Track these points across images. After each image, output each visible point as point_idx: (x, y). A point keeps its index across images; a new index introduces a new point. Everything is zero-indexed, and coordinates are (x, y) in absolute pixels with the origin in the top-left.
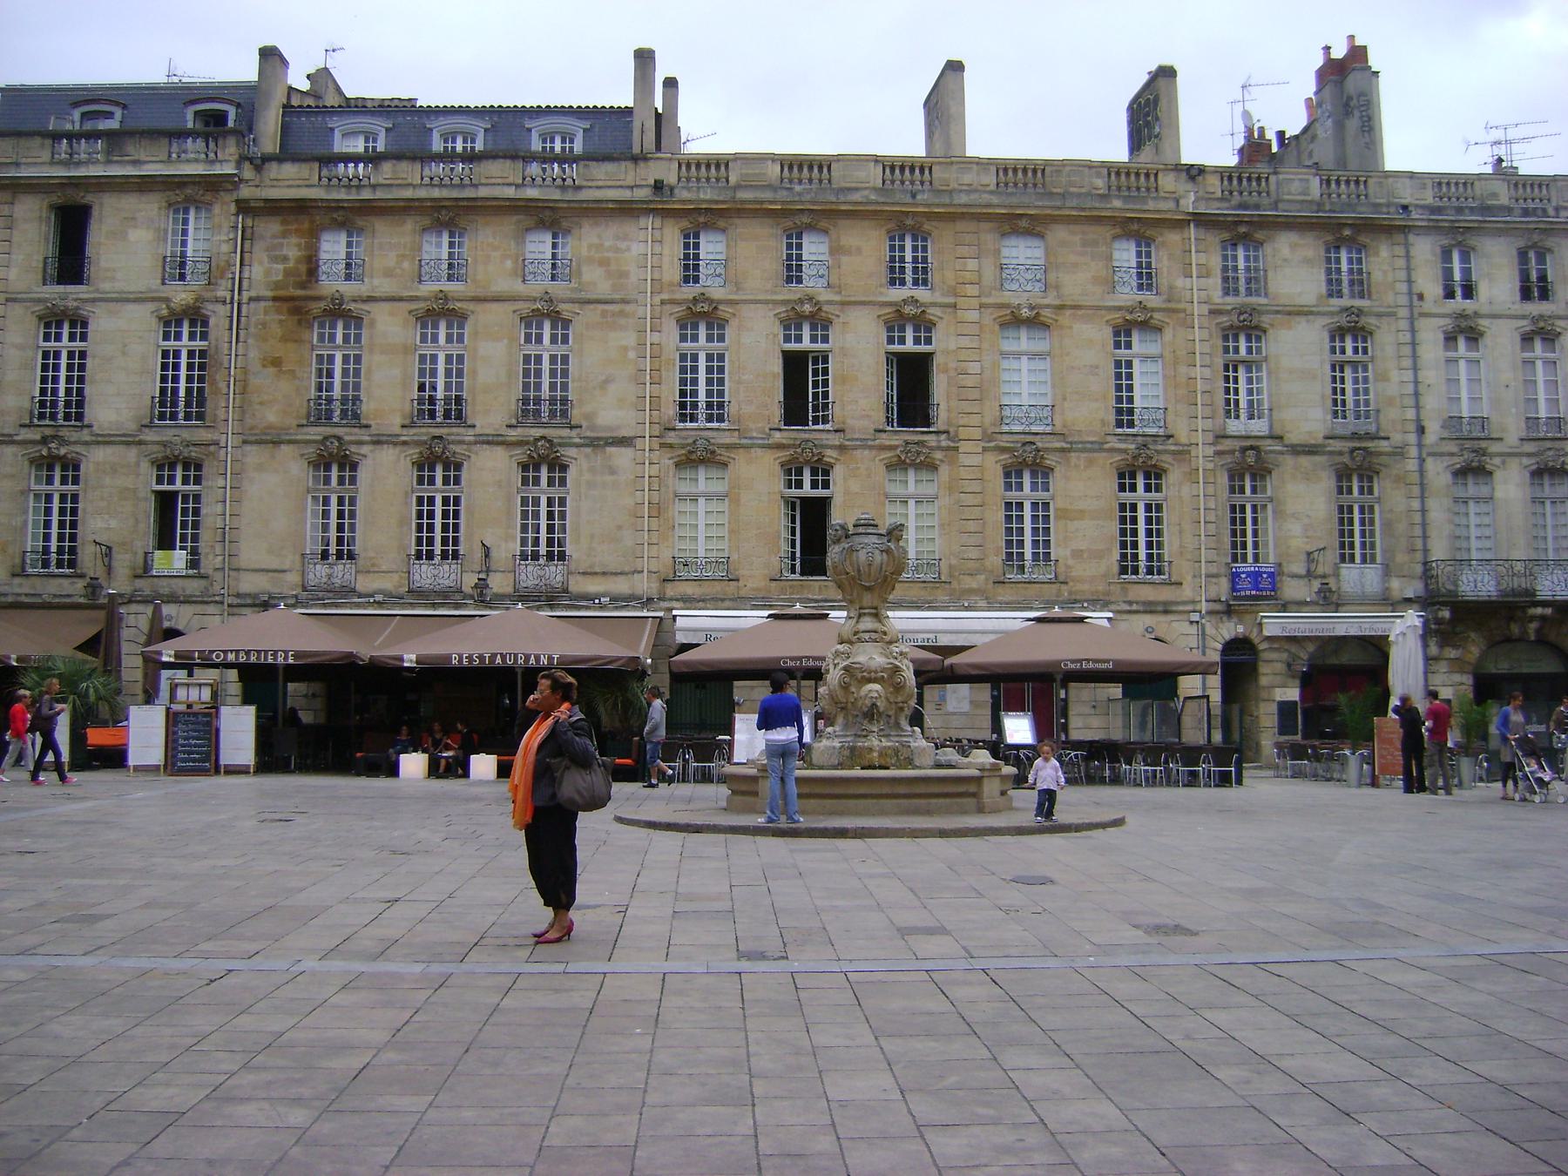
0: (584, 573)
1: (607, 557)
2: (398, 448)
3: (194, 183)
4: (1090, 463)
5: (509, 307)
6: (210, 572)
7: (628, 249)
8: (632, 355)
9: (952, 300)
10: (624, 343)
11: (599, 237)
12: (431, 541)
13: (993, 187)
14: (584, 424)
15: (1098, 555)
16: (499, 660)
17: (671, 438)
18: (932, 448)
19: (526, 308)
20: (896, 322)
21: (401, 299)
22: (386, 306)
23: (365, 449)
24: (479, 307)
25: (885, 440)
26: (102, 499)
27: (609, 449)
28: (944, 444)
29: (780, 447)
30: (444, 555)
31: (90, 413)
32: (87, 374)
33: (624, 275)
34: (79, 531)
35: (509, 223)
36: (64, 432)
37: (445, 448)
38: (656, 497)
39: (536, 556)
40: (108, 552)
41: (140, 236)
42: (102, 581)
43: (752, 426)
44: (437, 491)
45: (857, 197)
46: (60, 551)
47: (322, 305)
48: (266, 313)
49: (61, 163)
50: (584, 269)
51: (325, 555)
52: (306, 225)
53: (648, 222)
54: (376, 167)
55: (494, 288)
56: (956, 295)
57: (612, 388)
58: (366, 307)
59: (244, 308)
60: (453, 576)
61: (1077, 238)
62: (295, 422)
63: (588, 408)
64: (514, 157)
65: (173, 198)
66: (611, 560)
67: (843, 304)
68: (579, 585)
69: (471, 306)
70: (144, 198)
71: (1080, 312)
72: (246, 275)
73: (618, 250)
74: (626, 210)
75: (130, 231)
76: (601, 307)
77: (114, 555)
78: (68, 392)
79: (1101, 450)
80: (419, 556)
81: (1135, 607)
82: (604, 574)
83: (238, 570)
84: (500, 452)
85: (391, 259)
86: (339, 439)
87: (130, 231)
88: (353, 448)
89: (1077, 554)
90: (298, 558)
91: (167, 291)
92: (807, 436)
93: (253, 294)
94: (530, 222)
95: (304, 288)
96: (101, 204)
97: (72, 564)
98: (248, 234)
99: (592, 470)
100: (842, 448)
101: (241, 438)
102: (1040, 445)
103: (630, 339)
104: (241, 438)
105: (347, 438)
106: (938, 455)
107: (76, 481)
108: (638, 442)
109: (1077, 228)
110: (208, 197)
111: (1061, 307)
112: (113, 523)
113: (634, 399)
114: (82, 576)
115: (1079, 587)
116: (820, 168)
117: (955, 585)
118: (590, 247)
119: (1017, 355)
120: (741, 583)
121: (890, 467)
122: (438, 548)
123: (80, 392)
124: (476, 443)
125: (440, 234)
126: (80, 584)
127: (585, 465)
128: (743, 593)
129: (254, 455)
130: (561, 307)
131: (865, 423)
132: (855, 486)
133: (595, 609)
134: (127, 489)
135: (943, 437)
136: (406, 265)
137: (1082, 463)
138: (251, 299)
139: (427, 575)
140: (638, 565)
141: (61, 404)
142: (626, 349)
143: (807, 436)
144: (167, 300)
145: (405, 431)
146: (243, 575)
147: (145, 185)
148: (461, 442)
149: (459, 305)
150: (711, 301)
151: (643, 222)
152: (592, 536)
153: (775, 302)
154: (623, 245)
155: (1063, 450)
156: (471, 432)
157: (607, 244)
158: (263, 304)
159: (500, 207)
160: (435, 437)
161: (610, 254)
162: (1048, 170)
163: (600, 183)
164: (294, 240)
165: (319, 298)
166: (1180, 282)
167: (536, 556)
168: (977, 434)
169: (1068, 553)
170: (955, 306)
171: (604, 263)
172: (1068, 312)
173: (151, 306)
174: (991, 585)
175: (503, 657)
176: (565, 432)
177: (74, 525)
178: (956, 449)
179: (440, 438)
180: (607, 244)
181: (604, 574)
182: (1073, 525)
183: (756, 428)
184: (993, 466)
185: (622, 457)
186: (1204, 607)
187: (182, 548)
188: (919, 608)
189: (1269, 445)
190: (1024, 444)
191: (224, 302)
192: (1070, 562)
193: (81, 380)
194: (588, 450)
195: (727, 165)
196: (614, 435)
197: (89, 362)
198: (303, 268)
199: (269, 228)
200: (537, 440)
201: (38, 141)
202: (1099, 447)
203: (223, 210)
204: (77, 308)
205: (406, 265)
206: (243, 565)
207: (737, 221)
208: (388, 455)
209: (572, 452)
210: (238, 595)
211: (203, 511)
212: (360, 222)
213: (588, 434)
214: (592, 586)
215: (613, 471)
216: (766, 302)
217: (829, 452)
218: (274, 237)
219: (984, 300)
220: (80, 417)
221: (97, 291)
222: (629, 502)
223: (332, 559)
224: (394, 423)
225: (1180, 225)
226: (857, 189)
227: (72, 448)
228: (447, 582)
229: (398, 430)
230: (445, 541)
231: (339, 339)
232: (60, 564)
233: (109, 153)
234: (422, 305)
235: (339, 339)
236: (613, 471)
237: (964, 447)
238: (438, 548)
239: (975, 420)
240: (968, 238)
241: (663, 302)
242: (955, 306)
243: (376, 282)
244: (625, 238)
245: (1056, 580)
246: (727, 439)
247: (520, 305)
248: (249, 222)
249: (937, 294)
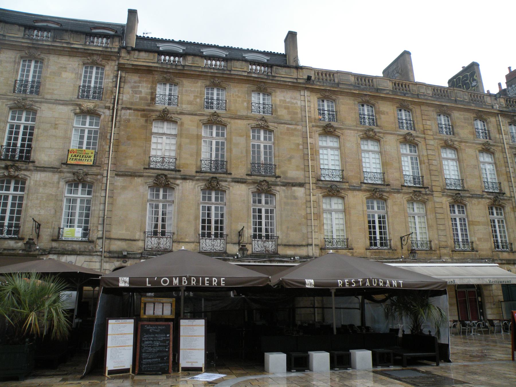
0: (285, 245)
1: (295, 237)
2: (194, 182)
3: (97, 54)
5: (245, 122)
6: (95, 239)
7: (297, 103)
8: (301, 147)
9: (423, 136)
10: (297, 142)
11: (284, 97)
12: (209, 228)
13: (431, 95)
14: (282, 176)
16: (368, 284)
18: (423, 194)
19: (254, 123)
21: (196, 115)
22: (190, 117)
23: (178, 182)
24: (232, 121)
26: (37, 199)
27: (294, 188)
28: (428, 192)
30: (216, 235)
31: (34, 156)
32: (34, 137)
33: (296, 113)
34: (22, 216)
35: (245, 87)
36: (19, 164)
37: (218, 183)
39: (260, 237)
40: (39, 226)
41: (68, 76)
42: (35, 240)
43: (353, 181)
44: (213, 204)
46: (10, 226)
47: (158, 114)
48: (130, 115)
49: (27, 39)
50: (278, 110)
51: (155, 233)
52: (151, 79)
54: (184, 59)
55: (239, 114)
56: (424, 134)
57: (293, 161)
58: (179, 116)
59: (119, 112)
60: (222, 245)
61: (462, 117)
62: (143, 167)
63: (283, 169)
64: (155, 52)
65: (86, 61)
67: (384, 133)
68: (282, 251)
69: (229, 120)
70: (71, 59)
71: (467, 144)
72: (121, 98)
73: (292, 103)
75: (63, 73)
76: (287, 126)
77: (41, 229)
78: (22, 145)
79: (482, 198)
80: (203, 235)
81: (503, 262)
82: (294, 246)
83: (110, 239)
84: (243, 187)
85: (191, 98)
86: (166, 176)
87: (63, 73)
88: (172, 181)
89: (479, 239)
90: (142, 234)
91: (80, 102)
92: (376, 186)
93: (124, 106)
94: (254, 88)
95: (149, 106)
96: (49, 59)
97: (16, 232)
98: (123, 80)
99: (286, 197)
101: (115, 173)
102: (462, 195)
103: (300, 141)
104: (115, 173)
105: (169, 176)
107: (23, 189)
108: (307, 186)
109: (462, 113)
110: (104, 62)
111: (461, 142)
112: (42, 212)
113: (303, 167)
114: (22, 239)
116: (330, 75)
117: (438, 252)
118: (280, 101)
119: (368, 151)
120: (354, 251)
122: (213, 232)
123: (29, 146)
124: (232, 181)
125: (165, 84)
126: (20, 244)
127: (283, 195)
129: (120, 181)
131: (397, 182)
132: (396, 209)
133: (291, 262)
134: (51, 194)
135: (427, 190)
136: (198, 100)
137: (476, 203)
138: (122, 108)
139: (207, 244)
140: (310, 242)
141: (18, 151)
142: (298, 145)
143: (376, 186)
144: (80, 105)
145: (198, 174)
146: (113, 242)
147: (73, 53)
148: (226, 181)
149: (223, 119)
150: (375, 132)
151: (302, 93)
152: (288, 228)
153: (358, 130)
154: (295, 101)
155: (469, 197)
156: (229, 176)
157: (287, 100)
158: (128, 111)
159: (279, 84)
160: (213, 178)
161: (289, 105)
162: (374, 80)
163: (283, 76)
164: (145, 85)
165: (156, 111)
166: (498, 136)
167: (260, 237)
169: (476, 239)
171: (287, 108)
172: (463, 144)
173: (71, 107)
174: (451, 253)
175: (371, 282)
176: (273, 179)
177: (19, 212)
178: (432, 195)
179: (216, 178)
180: (287, 100)
181: (294, 246)
182: (476, 228)
184: (446, 201)
185: (300, 192)
187: (79, 227)
188: (426, 262)
189: (462, 194)
190: (456, 194)
191: (109, 108)
192: (478, 243)
193: (30, 140)
194: (284, 188)
195: (333, 75)
196: (295, 181)
197: (36, 131)
198: (149, 97)
199: (133, 78)
200: (261, 181)
201: (17, 27)
202: (482, 197)
203: (110, 68)
204: (32, 105)
205: (198, 100)
206: (113, 236)
207: (340, 97)
208: (189, 185)
209: (278, 188)
210: (110, 252)
211: (92, 208)
212: (177, 80)
213: (284, 180)
214: (290, 252)
216: (354, 130)
217: (385, 194)
218: (135, 82)
219: (435, 137)
220: (28, 158)
221: (43, 98)
222: (303, 213)
223: (159, 235)
224: (191, 171)
225: (495, 115)
226: (384, 90)
227: (23, 172)
228: (219, 248)
229: (194, 174)
230: (216, 228)
231: (262, 138)
232: (9, 232)
233: (54, 38)
234: (206, 118)
235: (262, 138)
236: (295, 198)
237: (435, 194)
238: (213, 232)
241: (313, 126)
242: (425, 138)
243: (184, 106)
244: (295, 99)
245: (473, 250)
247: (251, 122)
248: (124, 75)
249: (418, 133)
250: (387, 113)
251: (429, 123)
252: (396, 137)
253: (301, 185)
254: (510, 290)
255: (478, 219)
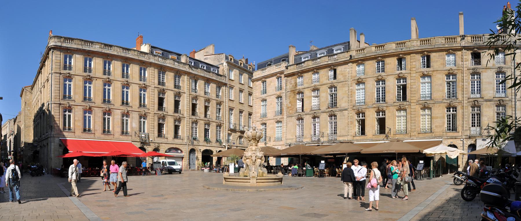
1: (344, 133)
4: (439, 106)
13: (419, 45)
15: (440, 126)
17: (355, 108)
20: (399, 78)
25: (396, 104)
29: (375, 107)
38: (352, 120)
45: (390, 52)
53: (350, 64)
66: (345, 134)
74: (345, 63)
89: (436, 126)
100: (387, 107)
103: (347, 89)
106: (407, 106)
111: (434, 71)
115: (437, 134)
121: (397, 110)
128: (368, 138)
130: (335, 84)
168: (415, 101)
170: (410, 73)
171: (342, 74)
176: (336, 109)
183: (370, 104)
185: (346, 112)
186: (464, 137)
209: (337, 113)
215: (344, 116)
237: (412, 104)
239: (414, 98)
240: (413, 58)
242: (410, 73)
246: (364, 107)
250: (390, 63)
251: (414, 63)
252: (394, 76)
253: (346, 110)
254: (518, 158)
255: (437, 115)
